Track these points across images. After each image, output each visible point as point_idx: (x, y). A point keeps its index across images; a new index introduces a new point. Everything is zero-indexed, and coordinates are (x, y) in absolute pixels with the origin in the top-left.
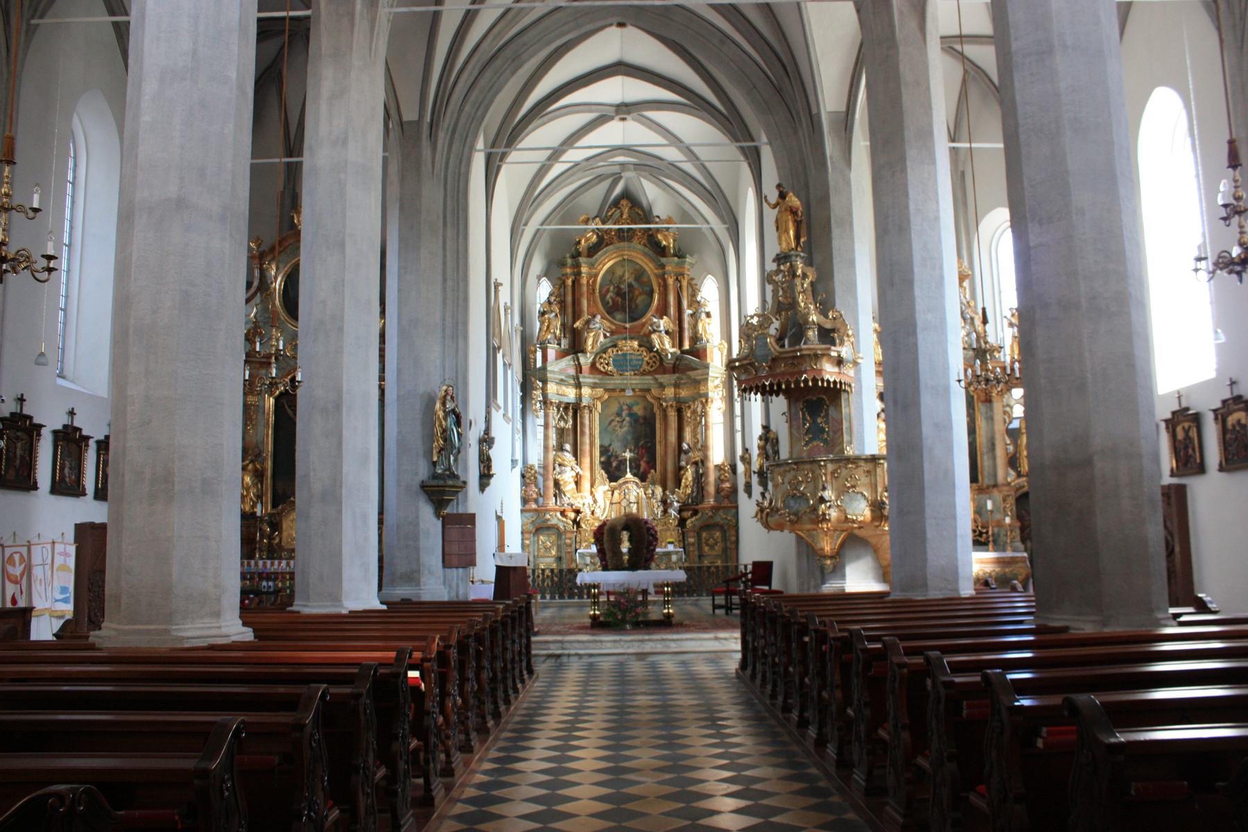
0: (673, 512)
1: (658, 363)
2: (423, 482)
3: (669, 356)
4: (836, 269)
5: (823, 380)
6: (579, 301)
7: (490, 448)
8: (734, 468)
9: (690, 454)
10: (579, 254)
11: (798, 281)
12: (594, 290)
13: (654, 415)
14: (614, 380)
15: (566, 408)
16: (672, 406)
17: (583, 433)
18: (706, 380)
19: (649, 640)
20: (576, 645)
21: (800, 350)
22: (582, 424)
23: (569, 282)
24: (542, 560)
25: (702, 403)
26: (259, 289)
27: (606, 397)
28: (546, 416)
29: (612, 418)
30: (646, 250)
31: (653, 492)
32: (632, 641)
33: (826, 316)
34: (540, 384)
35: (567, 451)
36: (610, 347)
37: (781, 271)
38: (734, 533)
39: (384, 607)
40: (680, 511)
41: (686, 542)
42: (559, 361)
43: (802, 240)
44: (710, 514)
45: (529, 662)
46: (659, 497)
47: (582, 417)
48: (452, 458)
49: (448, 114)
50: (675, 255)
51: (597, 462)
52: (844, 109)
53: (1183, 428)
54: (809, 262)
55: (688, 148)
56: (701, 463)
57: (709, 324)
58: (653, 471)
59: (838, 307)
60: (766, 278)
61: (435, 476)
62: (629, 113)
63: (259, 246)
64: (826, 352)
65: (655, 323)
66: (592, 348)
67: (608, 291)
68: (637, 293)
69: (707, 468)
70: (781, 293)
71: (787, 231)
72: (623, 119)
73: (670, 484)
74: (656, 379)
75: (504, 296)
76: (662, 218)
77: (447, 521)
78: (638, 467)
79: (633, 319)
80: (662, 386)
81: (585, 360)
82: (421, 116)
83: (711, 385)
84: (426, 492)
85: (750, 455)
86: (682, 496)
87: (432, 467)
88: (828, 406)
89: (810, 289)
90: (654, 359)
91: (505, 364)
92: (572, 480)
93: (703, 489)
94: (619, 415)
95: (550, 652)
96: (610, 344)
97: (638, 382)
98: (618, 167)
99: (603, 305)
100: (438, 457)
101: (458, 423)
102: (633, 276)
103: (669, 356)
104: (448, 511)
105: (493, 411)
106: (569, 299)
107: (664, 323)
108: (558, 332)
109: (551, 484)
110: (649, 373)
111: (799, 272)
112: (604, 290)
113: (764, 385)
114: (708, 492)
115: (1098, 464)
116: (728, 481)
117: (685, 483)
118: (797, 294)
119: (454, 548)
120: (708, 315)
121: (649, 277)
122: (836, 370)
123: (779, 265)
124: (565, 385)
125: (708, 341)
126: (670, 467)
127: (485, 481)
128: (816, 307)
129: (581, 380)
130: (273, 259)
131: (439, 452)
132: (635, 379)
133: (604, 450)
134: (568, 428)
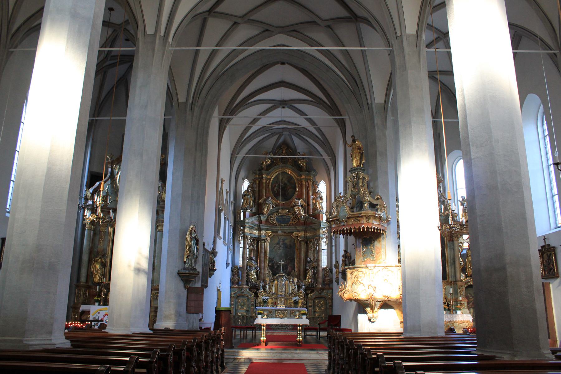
1: (297, 220)
2: (178, 271)
3: (303, 216)
7: (215, 256)
8: (331, 270)
9: (311, 263)
10: (262, 169)
11: (361, 181)
12: (269, 186)
14: (276, 227)
15: (254, 239)
16: (303, 240)
17: (261, 252)
18: (319, 229)
19: (285, 353)
21: (361, 214)
22: (261, 247)
23: (257, 181)
24: (239, 311)
25: (317, 240)
26: (110, 177)
27: (273, 235)
28: (244, 243)
29: (275, 245)
30: (293, 168)
31: (293, 280)
34: (242, 228)
35: (253, 260)
36: (275, 212)
37: (353, 176)
38: (330, 301)
39: (151, 332)
40: (305, 290)
41: (308, 305)
42: (251, 218)
43: (363, 162)
44: (320, 292)
45: (222, 363)
46: (296, 284)
47: (261, 245)
49: (200, 100)
50: (306, 171)
53: (547, 254)
56: (317, 267)
57: (321, 203)
58: (293, 271)
59: (380, 194)
60: (346, 182)
61: (185, 269)
62: (286, 104)
63: (111, 158)
65: (296, 201)
66: (267, 212)
67: (275, 186)
68: (289, 187)
69: (319, 270)
72: (283, 107)
73: (302, 277)
75: (226, 187)
76: (301, 153)
77: (190, 291)
82: (187, 100)
83: (321, 231)
84: (180, 276)
85: (339, 264)
86: (307, 283)
87: (184, 265)
89: (366, 185)
90: (295, 218)
91: (225, 218)
94: (278, 244)
96: (275, 211)
97: (287, 229)
99: (272, 193)
100: (187, 259)
101: (197, 244)
102: (287, 180)
103: (303, 216)
104: (190, 285)
105: (218, 239)
106: (257, 189)
107: (300, 202)
109: (245, 275)
112: (273, 186)
113: (343, 230)
115: (509, 269)
116: (328, 276)
117: (308, 277)
118: (360, 187)
120: (321, 198)
122: (378, 223)
124: (254, 229)
125: (321, 211)
126: (302, 269)
127: (212, 272)
128: (369, 193)
129: (261, 227)
130: (117, 164)
131: (187, 257)
132: (287, 228)
133: (271, 260)
134: (254, 250)
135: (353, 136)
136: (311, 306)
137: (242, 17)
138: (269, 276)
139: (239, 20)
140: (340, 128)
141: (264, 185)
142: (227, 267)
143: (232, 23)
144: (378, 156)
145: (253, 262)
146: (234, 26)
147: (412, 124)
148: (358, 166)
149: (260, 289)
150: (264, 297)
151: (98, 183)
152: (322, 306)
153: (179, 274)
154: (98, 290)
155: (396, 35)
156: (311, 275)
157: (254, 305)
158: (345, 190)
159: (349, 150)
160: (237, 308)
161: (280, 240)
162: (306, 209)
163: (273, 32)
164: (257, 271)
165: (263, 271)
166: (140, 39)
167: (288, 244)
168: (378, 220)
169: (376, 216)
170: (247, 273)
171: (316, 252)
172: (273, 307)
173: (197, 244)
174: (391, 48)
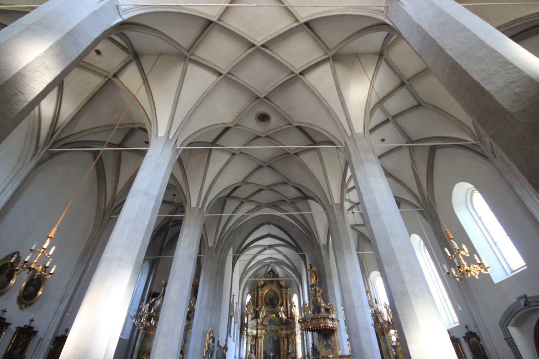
3: (284, 319)
5: (328, 326)
7: (226, 351)
11: (317, 293)
13: (280, 340)
16: (285, 337)
17: (258, 346)
23: (256, 296)
33: (327, 304)
34: (246, 329)
37: (313, 290)
52: (326, 243)
54: (320, 286)
59: (330, 301)
60: (309, 294)
62: (271, 247)
63: (165, 282)
65: (280, 309)
66: (262, 317)
67: (266, 299)
70: (313, 297)
71: (313, 278)
72: (270, 249)
75: (236, 300)
80: (282, 330)
81: (260, 321)
82: (214, 245)
83: (296, 329)
88: (331, 336)
91: (235, 322)
94: (269, 340)
101: (213, 342)
105: (229, 338)
106: (255, 301)
107: (282, 309)
108: (252, 311)
110: (279, 325)
111: (318, 290)
113: (310, 328)
120: (295, 306)
121: (278, 295)
123: (311, 288)
131: (206, 353)
133: (265, 353)
134: (253, 345)
135: (310, 265)
137: (246, 199)
139: (244, 201)
143: (240, 202)
144: (327, 276)
146: (241, 204)
148: (315, 283)
151: (153, 299)
155: (329, 204)
158: (309, 299)
159: (309, 273)
161: (270, 337)
162: (286, 315)
163: (262, 207)
168: (331, 320)
171: (294, 345)
173: (213, 342)
174: (327, 212)
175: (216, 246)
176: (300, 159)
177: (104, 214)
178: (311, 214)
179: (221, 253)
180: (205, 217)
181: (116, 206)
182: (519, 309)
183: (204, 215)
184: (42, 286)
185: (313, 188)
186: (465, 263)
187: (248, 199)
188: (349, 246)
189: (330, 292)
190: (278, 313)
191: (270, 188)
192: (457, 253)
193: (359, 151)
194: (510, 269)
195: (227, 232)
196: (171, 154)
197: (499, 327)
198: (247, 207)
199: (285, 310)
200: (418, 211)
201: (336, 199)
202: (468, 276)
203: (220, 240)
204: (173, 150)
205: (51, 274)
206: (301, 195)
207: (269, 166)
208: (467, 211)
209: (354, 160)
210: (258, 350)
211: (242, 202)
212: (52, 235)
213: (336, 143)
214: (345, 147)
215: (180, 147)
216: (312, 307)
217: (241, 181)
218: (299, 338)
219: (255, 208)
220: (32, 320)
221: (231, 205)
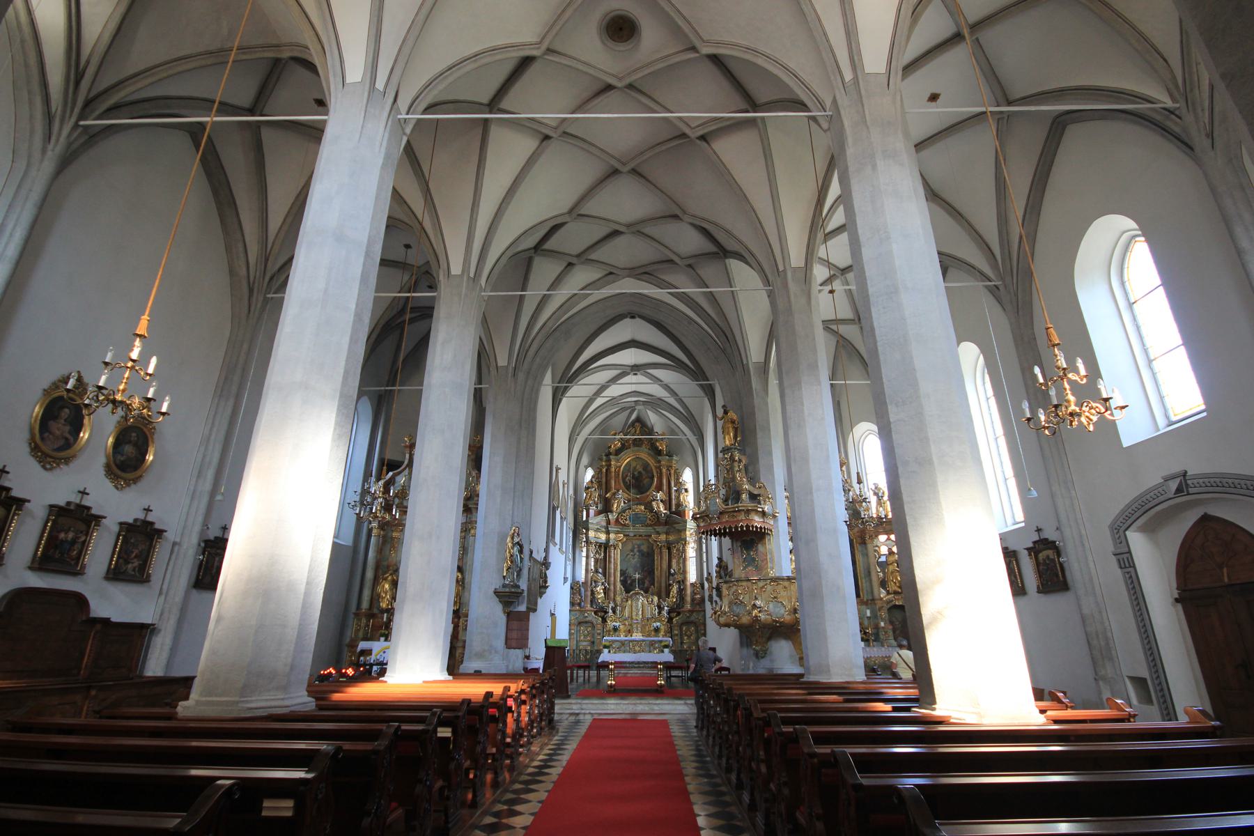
0: (665, 613)
2: (495, 589)
4: (760, 456)
5: (753, 526)
6: (610, 480)
7: (547, 569)
11: (736, 464)
12: (618, 475)
15: (600, 545)
17: (610, 562)
18: (685, 530)
19: (641, 704)
20: (590, 706)
21: (737, 507)
22: (610, 556)
23: (604, 470)
24: (581, 643)
26: (407, 466)
27: (625, 539)
28: (588, 551)
32: (628, 704)
34: (584, 531)
37: (726, 458)
38: (703, 628)
39: (451, 678)
40: (669, 613)
43: (739, 439)
44: (688, 615)
46: (656, 604)
48: (515, 574)
50: (667, 455)
51: (619, 580)
54: (742, 452)
55: (666, 385)
56: (683, 581)
58: (652, 587)
59: (762, 480)
60: (717, 466)
62: (638, 371)
64: (756, 508)
67: (627, 476)
68: (644, 477)
70: (726, 472)
71: (729, 434)
72: (636, 374)
73: (663, 595)
74: (655, 529)
75: (562, 476)
77: (509, 615)
78: (644, 583)
79: (642, 493)
80: (658, 533)
81: (612, 517)
83: (688, 533)
84: (496, 595)
88: (757, 544)
89: (743, 469)
91: (561, 518)
92: (602, 591)
93: (683, 599)
94: (632, 551)
95: (572, 711)
98: (633, 403)
101: (521, 552)
105: (551, 545)
106: (604, 480)
107: (659, 495)
108: (596, 499)
109: (589, 593)
110: (651, 526)
113: (715, 529)
114: (686, 600)
116: (699, 594)
119: (514, 634)
120: (686, 490)
122: (762, 520)
123: (724, 455)
127: (542, 590)
131: (507, 570)
133: (623, 573)
135: (724, 406)
136: (677, 635)
137: (578, 256)
138: (621, 594)
139: (574, 260)
140: (708, 399)
141: (613, 474)
142: (565, 582)
143: (565, 264)
145: (600, 575)
146: (568, 268)
147: (803, 384)
149: (608, 612)
150: (614, 623)
151: (391, 474)
152: (691, 635)
153: (496, 592)
154: (385, 620)
155: (778, 269)
156: (675, 592)
157: (602, 635)
158: (717, 476)
159: (720, 423)
160: (578, 639)
162: (668, 503)
163: (618, 275)
164: (605, 587)
165: (612, 587)
166: (442, 282)
167: (645, 550)
168: (761, 515)
169: (759, 509)
170: (592, 591)
171: (681, 561)
172: (626, 637)
173: (521, 552)
174: (771, 288)
175: (515, 365)
176: (715, 153)
177: (251, 291)
178: (732, 291)
179: (526, 382)
180: (486, 298)
181: (273, 272)
182: (1162, 498)
183: (483, 294)
184: (150, 443)
185: (742, 231)
186: (1072, 398)
187: (584, 257)
188: (814, 367)
189: (762, 462)
190: (650, 503)
191: (637, 228)
192: (1059, 377)
193: (868, 128)
194: (1167, 417)
195: (538, 333)
196: (387, 135)
197: (1108, 533)
198: (582, 276)
199: (664, 498)
200: (986, 287)
201: (796, 257)
202: (1071, 425)
203: (523, 352)
204: (390, 123)
205: (163, 414)
206: (711, 248)
207: (634, 171)
208: (1106, 287)
209: (850, 151)
210: (609, 568)
211: (570, 265)
212: (142, 328)
213: (809, 104)
214: (832, 116)
215: (407, 114)
216: (723, 492)
217: (565, 210)
218: (693, 548)
219: (599, 280)
220: (148, 510)
221: (545, 270)
